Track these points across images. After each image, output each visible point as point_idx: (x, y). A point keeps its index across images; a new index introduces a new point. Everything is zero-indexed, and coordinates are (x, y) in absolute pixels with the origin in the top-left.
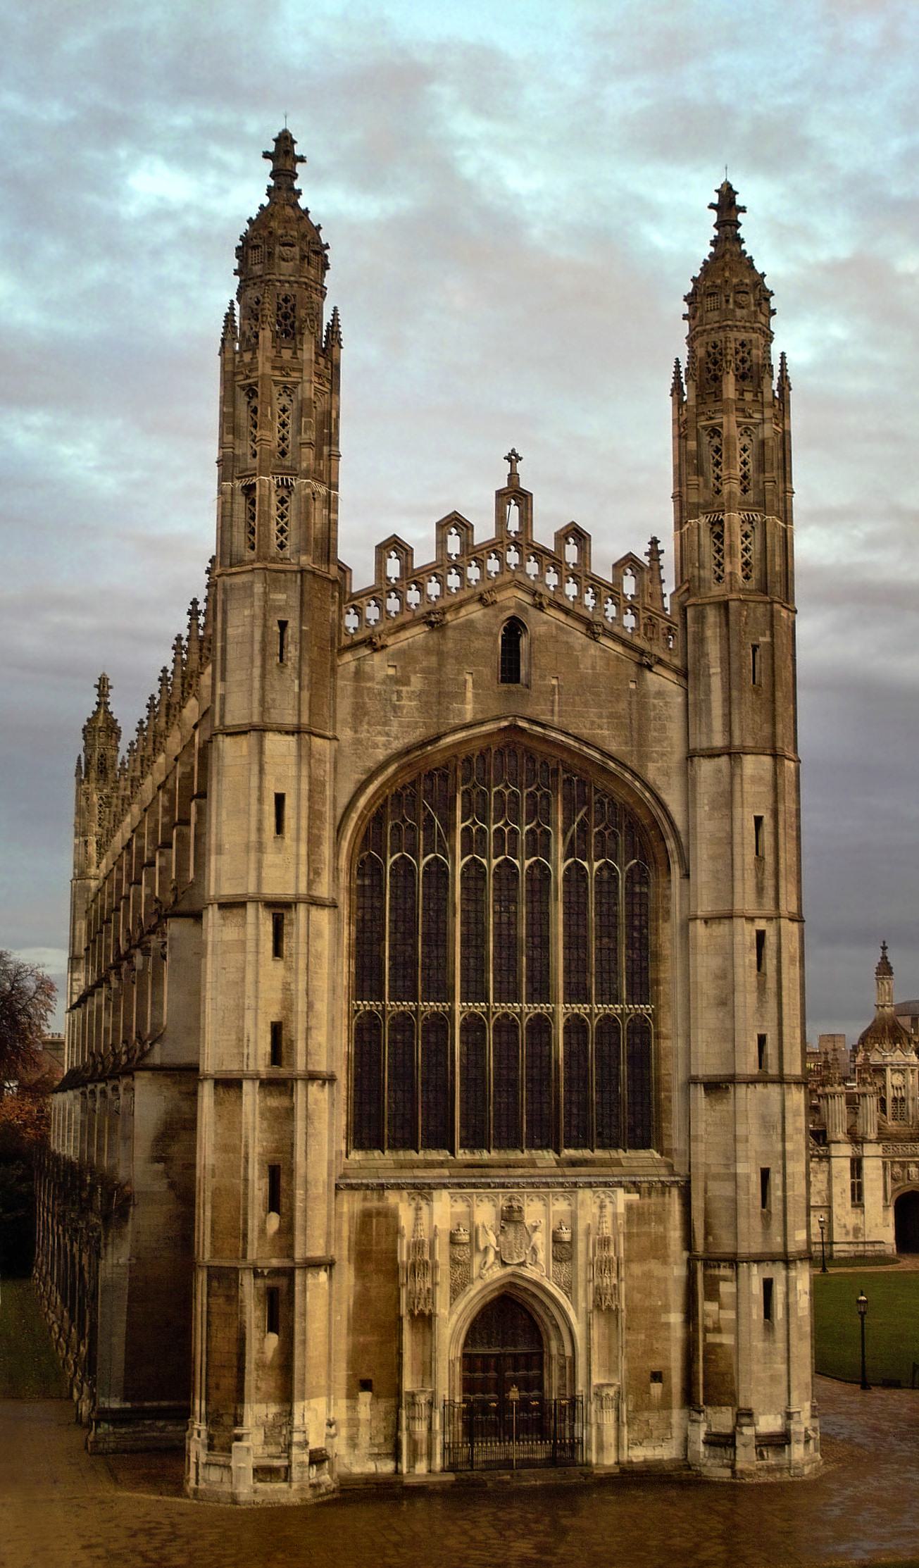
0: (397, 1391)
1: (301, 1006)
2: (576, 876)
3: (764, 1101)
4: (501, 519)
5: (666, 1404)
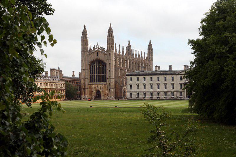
2: (102, 67)
4: (97, 47)
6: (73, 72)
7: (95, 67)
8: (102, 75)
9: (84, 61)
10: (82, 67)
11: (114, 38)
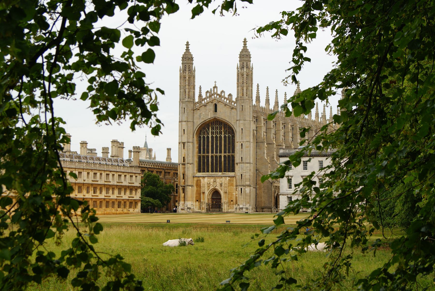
0: (200, 202)
1: (186, 155)
2: (225, 137)
3: (242, 166)
4: (214, 90)
5: (233, 204)
6: (169, 150)
7: (210, 136)
8: (225, 156)
9: (184, 123)
10: (181, 136)
11: (254, 70)
